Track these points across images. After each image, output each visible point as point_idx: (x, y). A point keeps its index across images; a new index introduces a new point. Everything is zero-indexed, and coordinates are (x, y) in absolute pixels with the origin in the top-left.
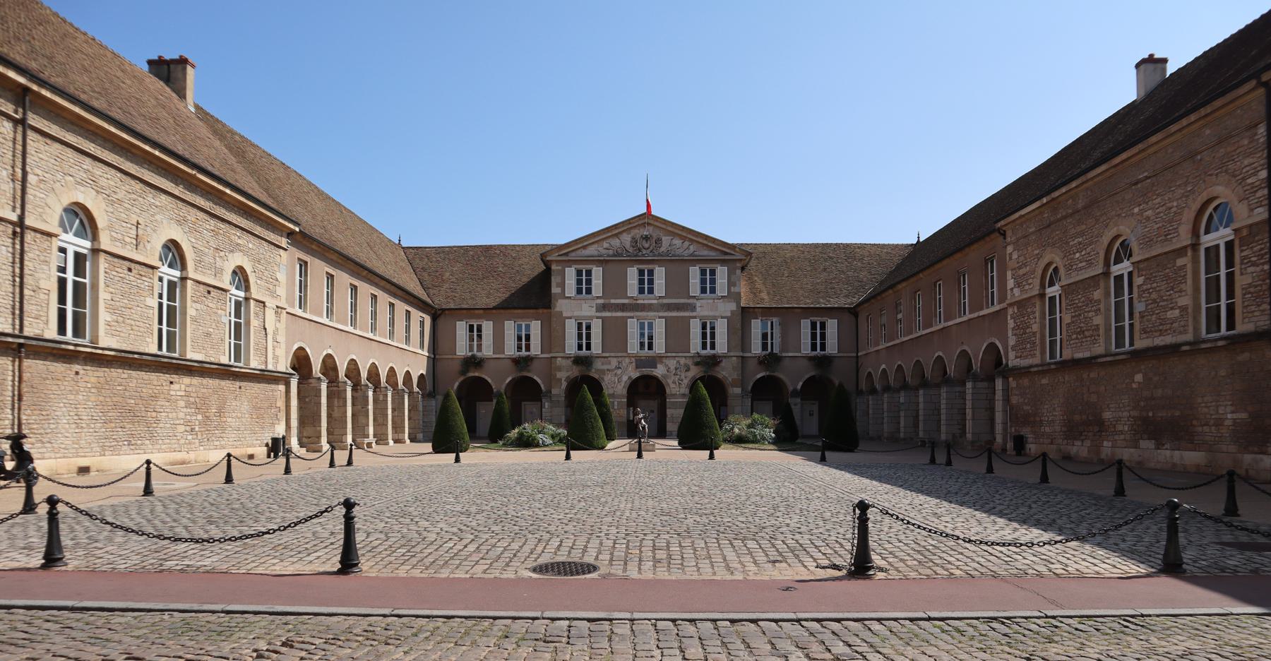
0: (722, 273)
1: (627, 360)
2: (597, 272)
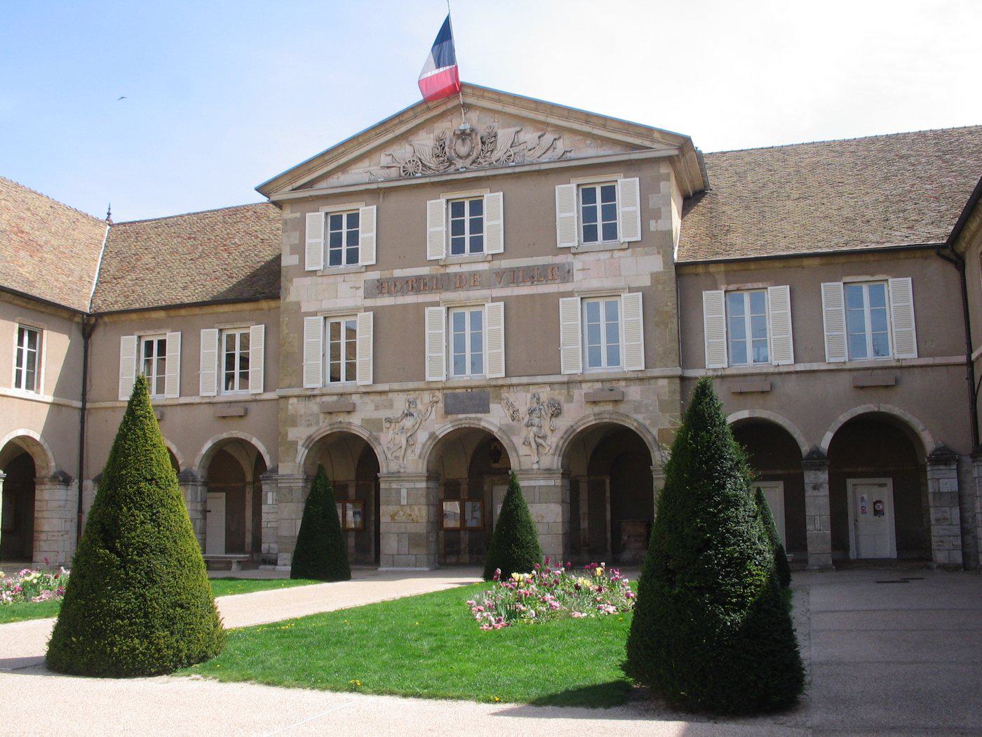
0: (628, 189)
1: (427, 397)
2: (368, 214)
